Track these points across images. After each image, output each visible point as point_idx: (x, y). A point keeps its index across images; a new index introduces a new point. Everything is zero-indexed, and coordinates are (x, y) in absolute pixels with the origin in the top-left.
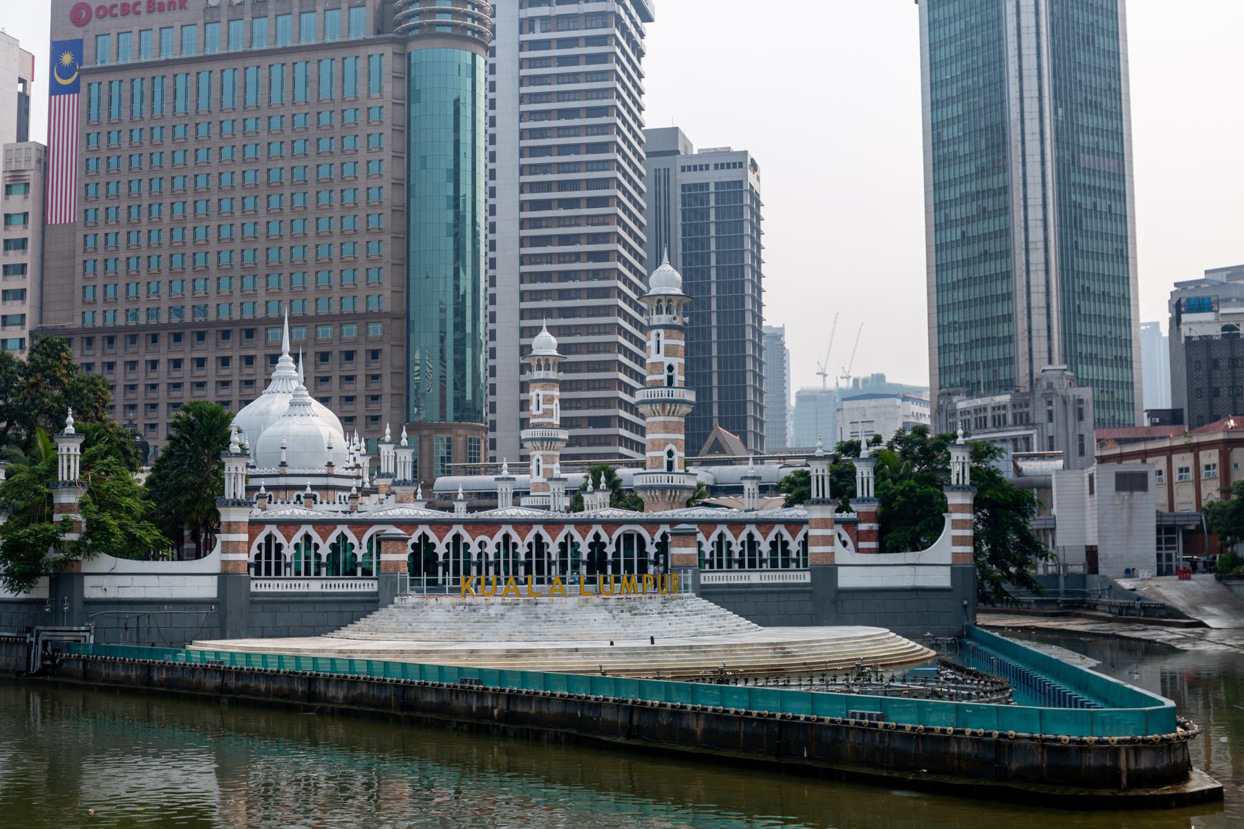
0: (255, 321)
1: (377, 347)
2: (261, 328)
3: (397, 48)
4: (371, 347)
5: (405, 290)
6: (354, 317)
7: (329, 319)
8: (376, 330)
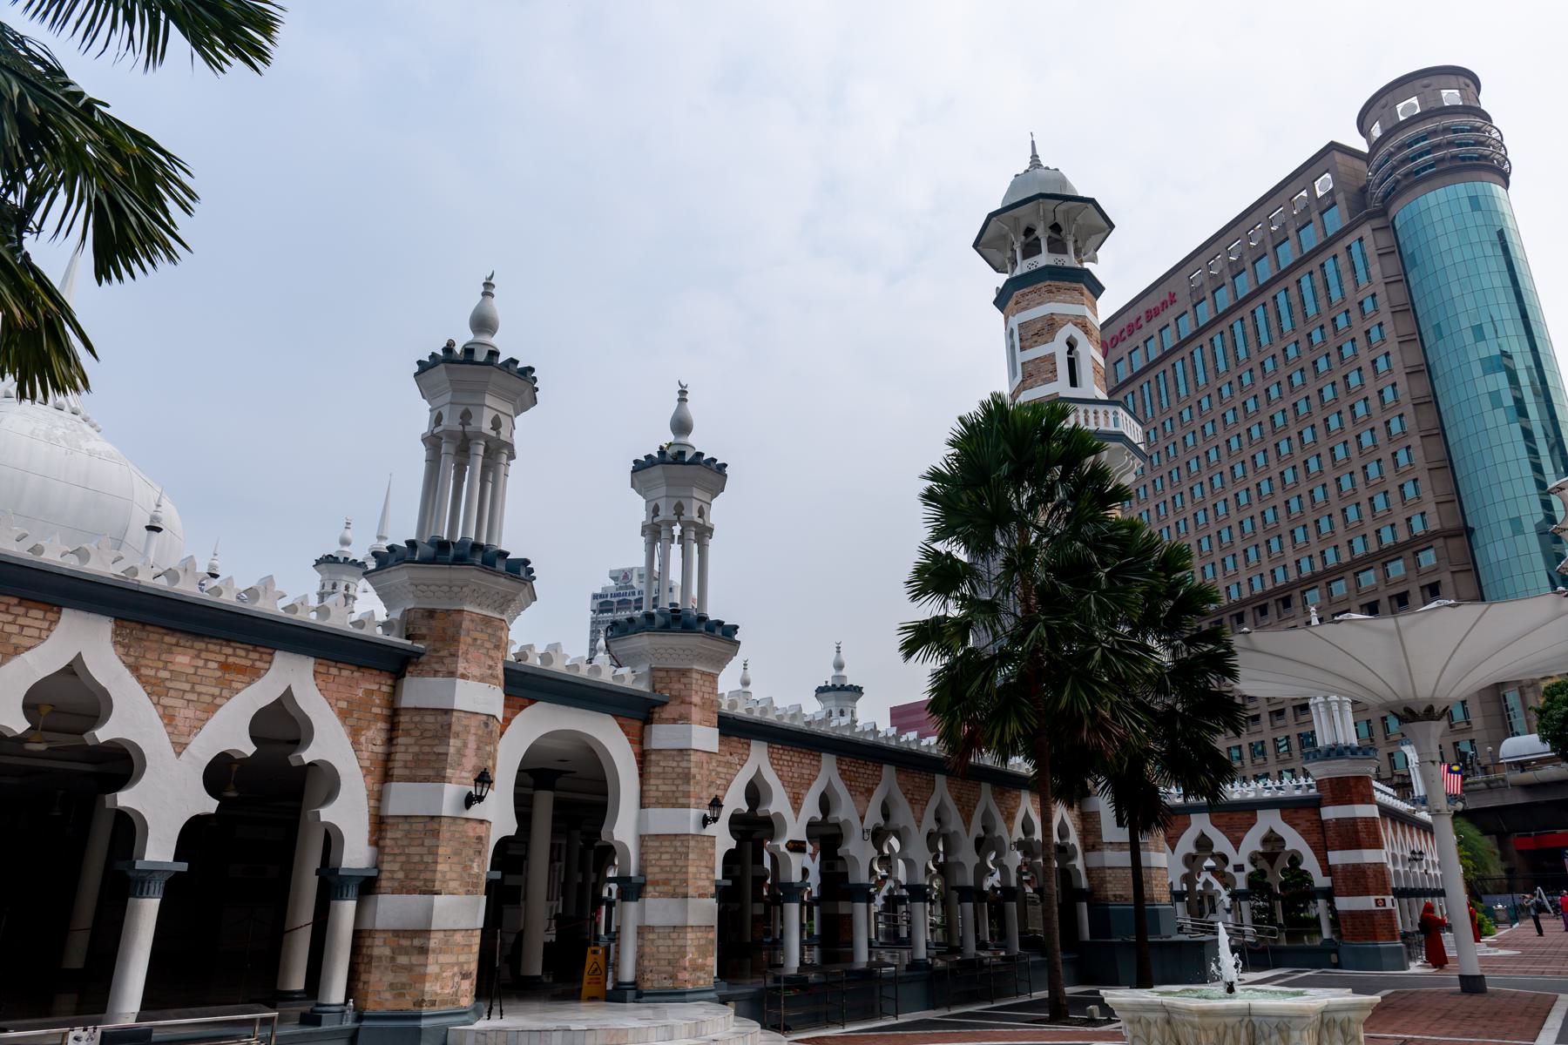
0: (1289, 586)
1: (1434, 579)
2: (1297, 593)
3: (1377, 223)
4: (1426, 581)
5: (1455, 498)
6: (1396, 551)
7: (1366, 562)
8: (1428, 559)
